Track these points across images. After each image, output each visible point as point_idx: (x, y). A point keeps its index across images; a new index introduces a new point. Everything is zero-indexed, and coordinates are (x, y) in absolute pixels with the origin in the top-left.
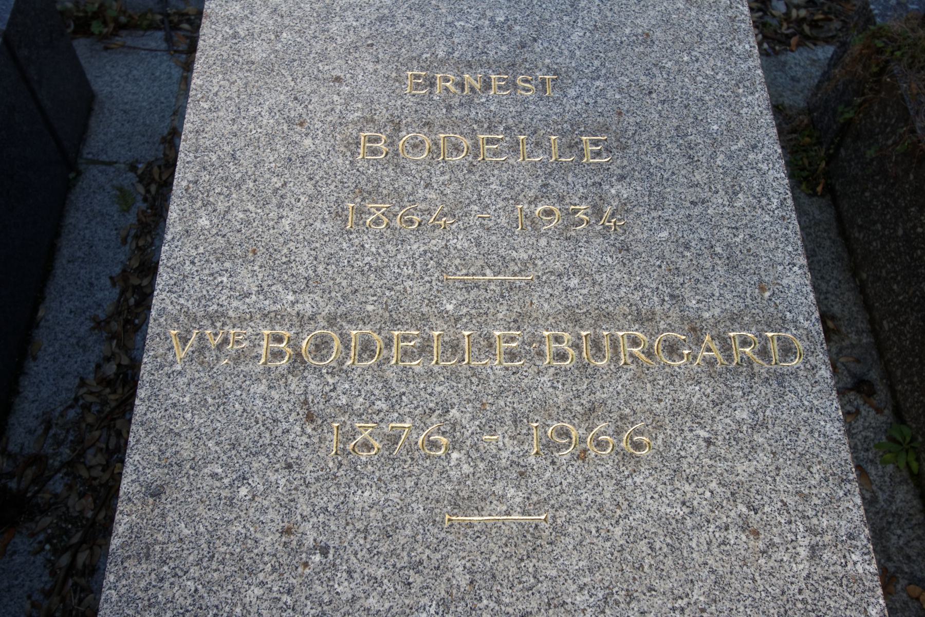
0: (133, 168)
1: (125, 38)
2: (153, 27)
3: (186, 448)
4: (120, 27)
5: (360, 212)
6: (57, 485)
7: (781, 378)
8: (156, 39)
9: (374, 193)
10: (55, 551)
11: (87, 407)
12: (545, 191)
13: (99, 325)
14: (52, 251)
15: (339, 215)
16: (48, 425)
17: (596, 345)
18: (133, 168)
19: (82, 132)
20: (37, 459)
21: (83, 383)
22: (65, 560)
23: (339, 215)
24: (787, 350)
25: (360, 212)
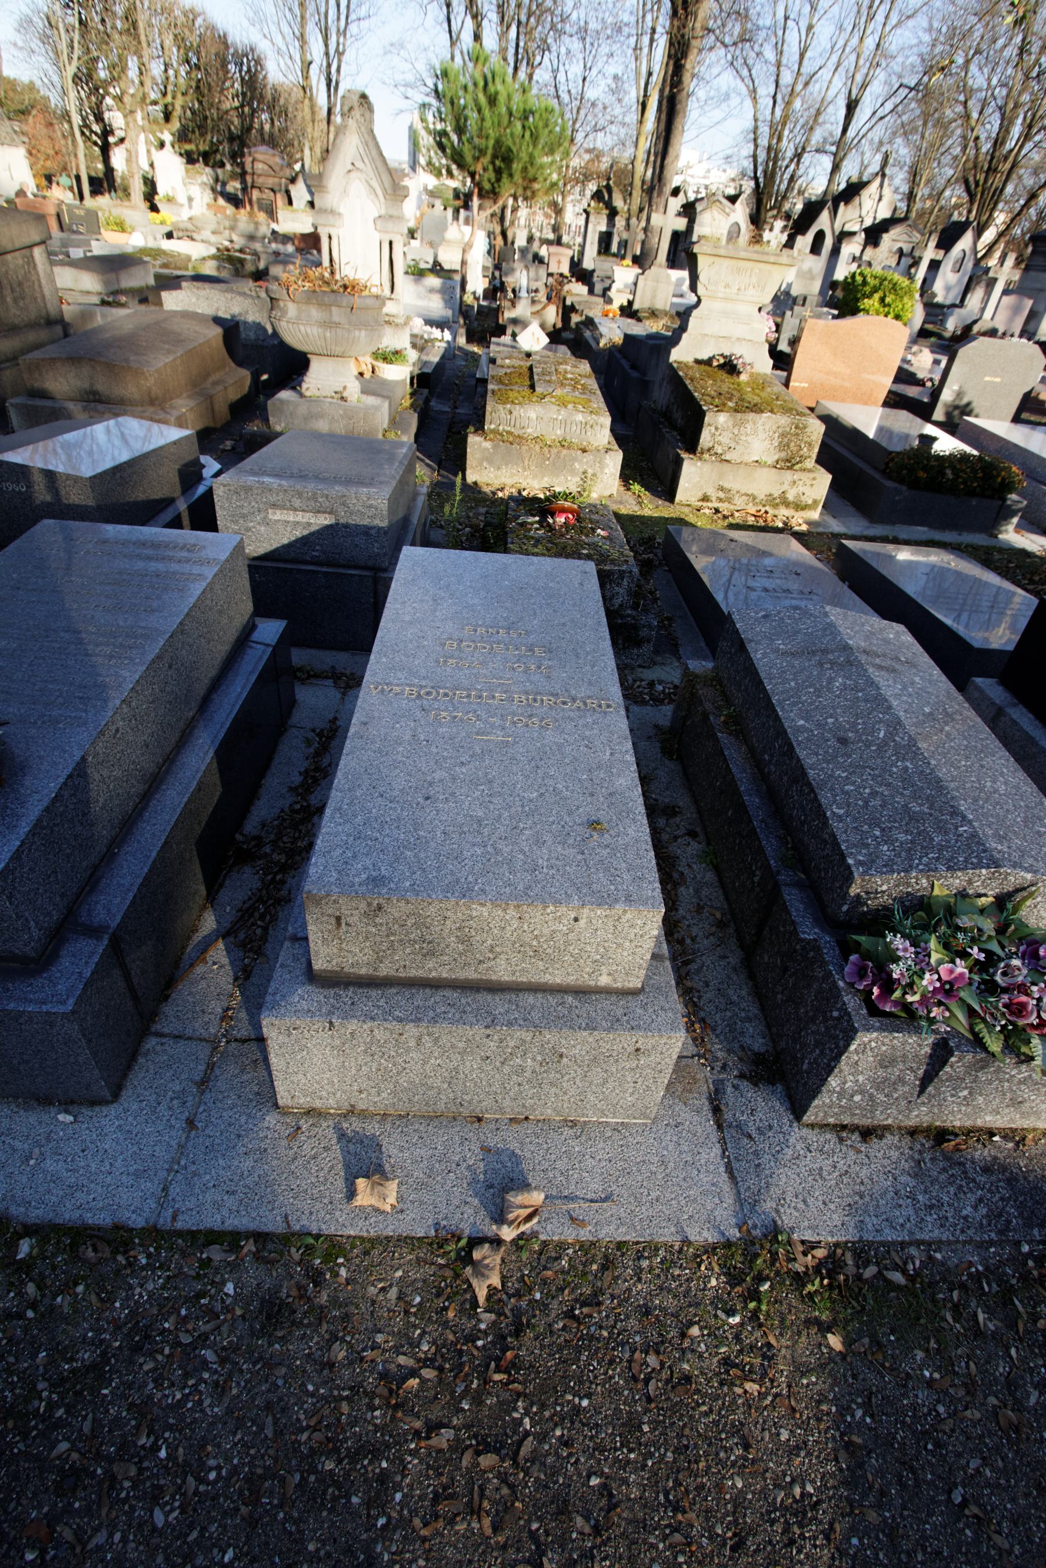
0: (313, 730)
1: (313, 680)
2: (327, 678)
3: (376, 714)
4: (309, 677)
5: (445, 662)
6: (267, 849)
7: (605, 713)
8: (330, 682)
9: (452, 657)
10: (264, 874)
11: (284, 820)
12: (518, 661)
13: (291, 789)
14: (270, 759)
15: (437, 661)
16: (263, 825)
17: (535, 700)
18: (313, 730)
19: (289, 714)
20: (258, 838)
21: (282, 811)
22: (269, 877)
23: (437, 661)
24: (609, 706)
25: (445, 662)
